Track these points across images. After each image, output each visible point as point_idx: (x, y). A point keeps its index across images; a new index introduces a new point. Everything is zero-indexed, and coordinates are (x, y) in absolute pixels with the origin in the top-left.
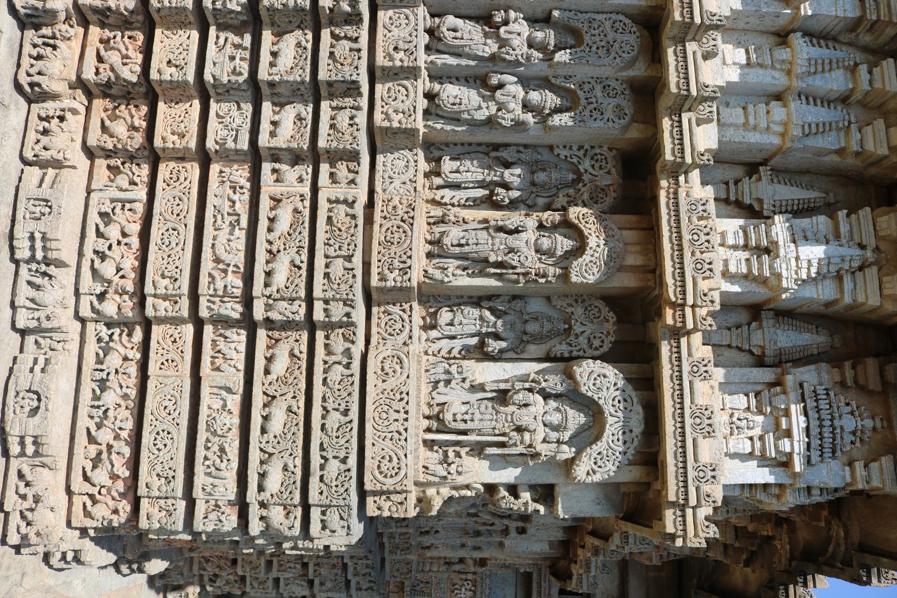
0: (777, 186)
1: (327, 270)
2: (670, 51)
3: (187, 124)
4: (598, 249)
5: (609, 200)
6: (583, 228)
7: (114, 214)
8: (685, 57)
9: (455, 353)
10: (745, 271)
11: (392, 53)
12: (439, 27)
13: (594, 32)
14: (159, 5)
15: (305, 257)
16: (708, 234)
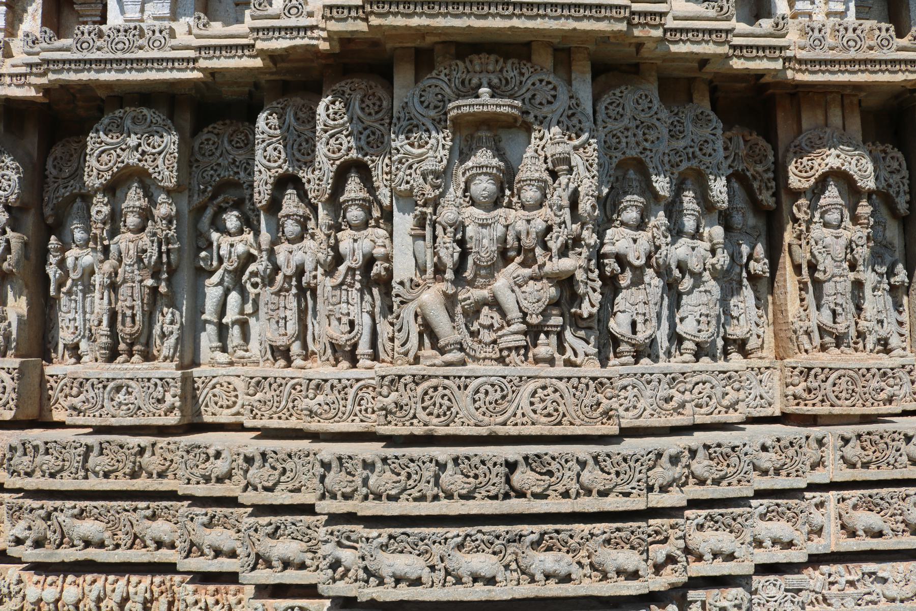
2: (674, 48)
4: (843, 156)
5: (762, 142)
6: (820, 172)
9: (900, 319)
11: (674, 404)
12: (633, 345)
13: (625, 144)
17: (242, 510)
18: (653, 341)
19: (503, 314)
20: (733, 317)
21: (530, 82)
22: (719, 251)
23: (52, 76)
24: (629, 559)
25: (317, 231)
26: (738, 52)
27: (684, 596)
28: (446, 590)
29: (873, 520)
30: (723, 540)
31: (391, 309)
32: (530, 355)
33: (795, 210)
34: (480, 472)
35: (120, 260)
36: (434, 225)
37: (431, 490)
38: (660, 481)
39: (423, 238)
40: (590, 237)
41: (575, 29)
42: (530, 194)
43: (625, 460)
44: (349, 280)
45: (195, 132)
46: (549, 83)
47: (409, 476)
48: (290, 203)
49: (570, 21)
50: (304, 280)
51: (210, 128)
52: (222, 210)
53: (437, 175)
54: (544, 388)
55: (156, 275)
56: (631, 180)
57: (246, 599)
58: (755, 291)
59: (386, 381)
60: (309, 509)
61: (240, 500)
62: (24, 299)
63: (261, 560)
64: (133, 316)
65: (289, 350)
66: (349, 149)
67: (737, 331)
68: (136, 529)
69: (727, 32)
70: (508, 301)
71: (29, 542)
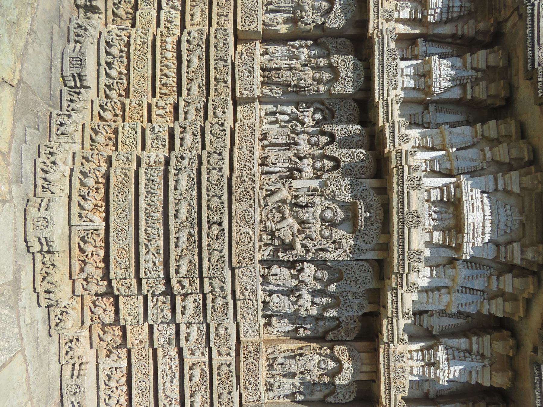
0: (442, 318)
1: (220, 400)
2: (389, 293)
3: (143, 336)
4: (349, 370)
5: (354, 335)
7: (112, 374)
8: (397, 297)
9: (281, 397)
10: (421, 374)
11: (244, 291)
12: (267, 275)
14: (119, 293)
15: (208, 394)
16: (403, 372)
17: (203, 122)
18: (269, 283)
19: (279, 222)
20: (280, 320)
21: (372, 233)
22: (306, 312)
23: (377, 40)
24: (184, 270)
25: (312, 150)
26: (390, 322)
27: (168, 295)
28: (173, 199)
29: (196, 378)
30: (190, 311)
31: (282, 179)
32: (263, 233)
33: (325, 348)
34: (218, 212)
35: (301, 71)
36: (314, 195)
37: (211, 193)
38: (214, 283)
39: (309, 191)
40: (309, 256)
41: (394, 250)
42: (326, 232)
43: (222, 268)
44: (293, 163)
45: (355, 100)
46: (372, 241)
47: (216, 185)
48: (324, 139)
49: (397, 249)
50: (293, 145)
51: (356, 106)
52: (322, 112)
53: (333, 196)
54: (250, 238)
55: (295, 86)
56: (334, 275)
57: (168, 124)
58: (291, 331)
59: (252, 177)
60: (203, 147)
61: (207, 121)
62: (286, 31)
63: (184, 130)
64: (279, 77)
65: (265, 140)
66: (345, 162)
67: (274, 321)
68: (195, 80)
69: (397, 316)
70: (284, 224)
71: (189, 38)
